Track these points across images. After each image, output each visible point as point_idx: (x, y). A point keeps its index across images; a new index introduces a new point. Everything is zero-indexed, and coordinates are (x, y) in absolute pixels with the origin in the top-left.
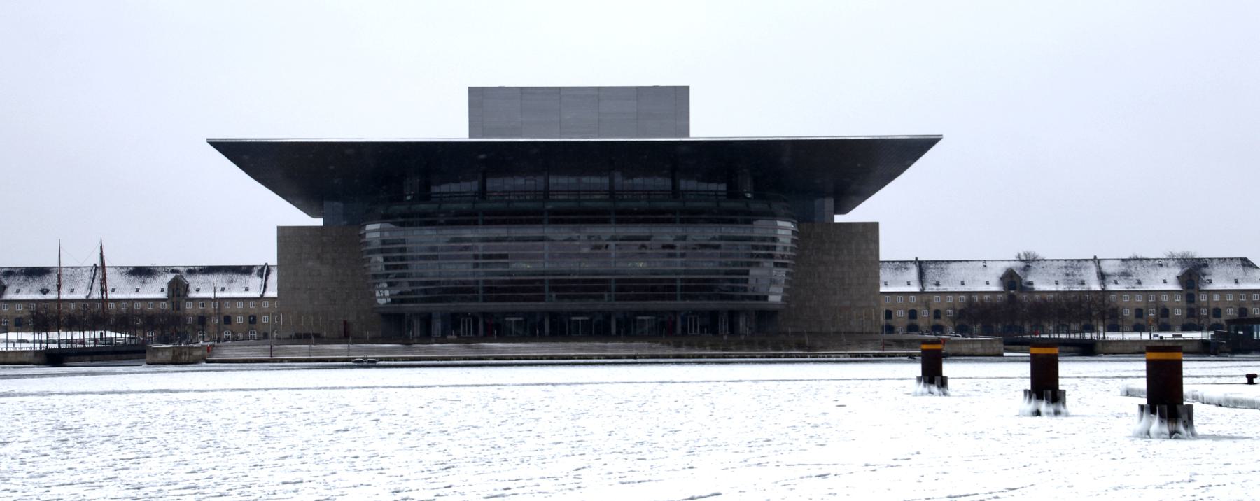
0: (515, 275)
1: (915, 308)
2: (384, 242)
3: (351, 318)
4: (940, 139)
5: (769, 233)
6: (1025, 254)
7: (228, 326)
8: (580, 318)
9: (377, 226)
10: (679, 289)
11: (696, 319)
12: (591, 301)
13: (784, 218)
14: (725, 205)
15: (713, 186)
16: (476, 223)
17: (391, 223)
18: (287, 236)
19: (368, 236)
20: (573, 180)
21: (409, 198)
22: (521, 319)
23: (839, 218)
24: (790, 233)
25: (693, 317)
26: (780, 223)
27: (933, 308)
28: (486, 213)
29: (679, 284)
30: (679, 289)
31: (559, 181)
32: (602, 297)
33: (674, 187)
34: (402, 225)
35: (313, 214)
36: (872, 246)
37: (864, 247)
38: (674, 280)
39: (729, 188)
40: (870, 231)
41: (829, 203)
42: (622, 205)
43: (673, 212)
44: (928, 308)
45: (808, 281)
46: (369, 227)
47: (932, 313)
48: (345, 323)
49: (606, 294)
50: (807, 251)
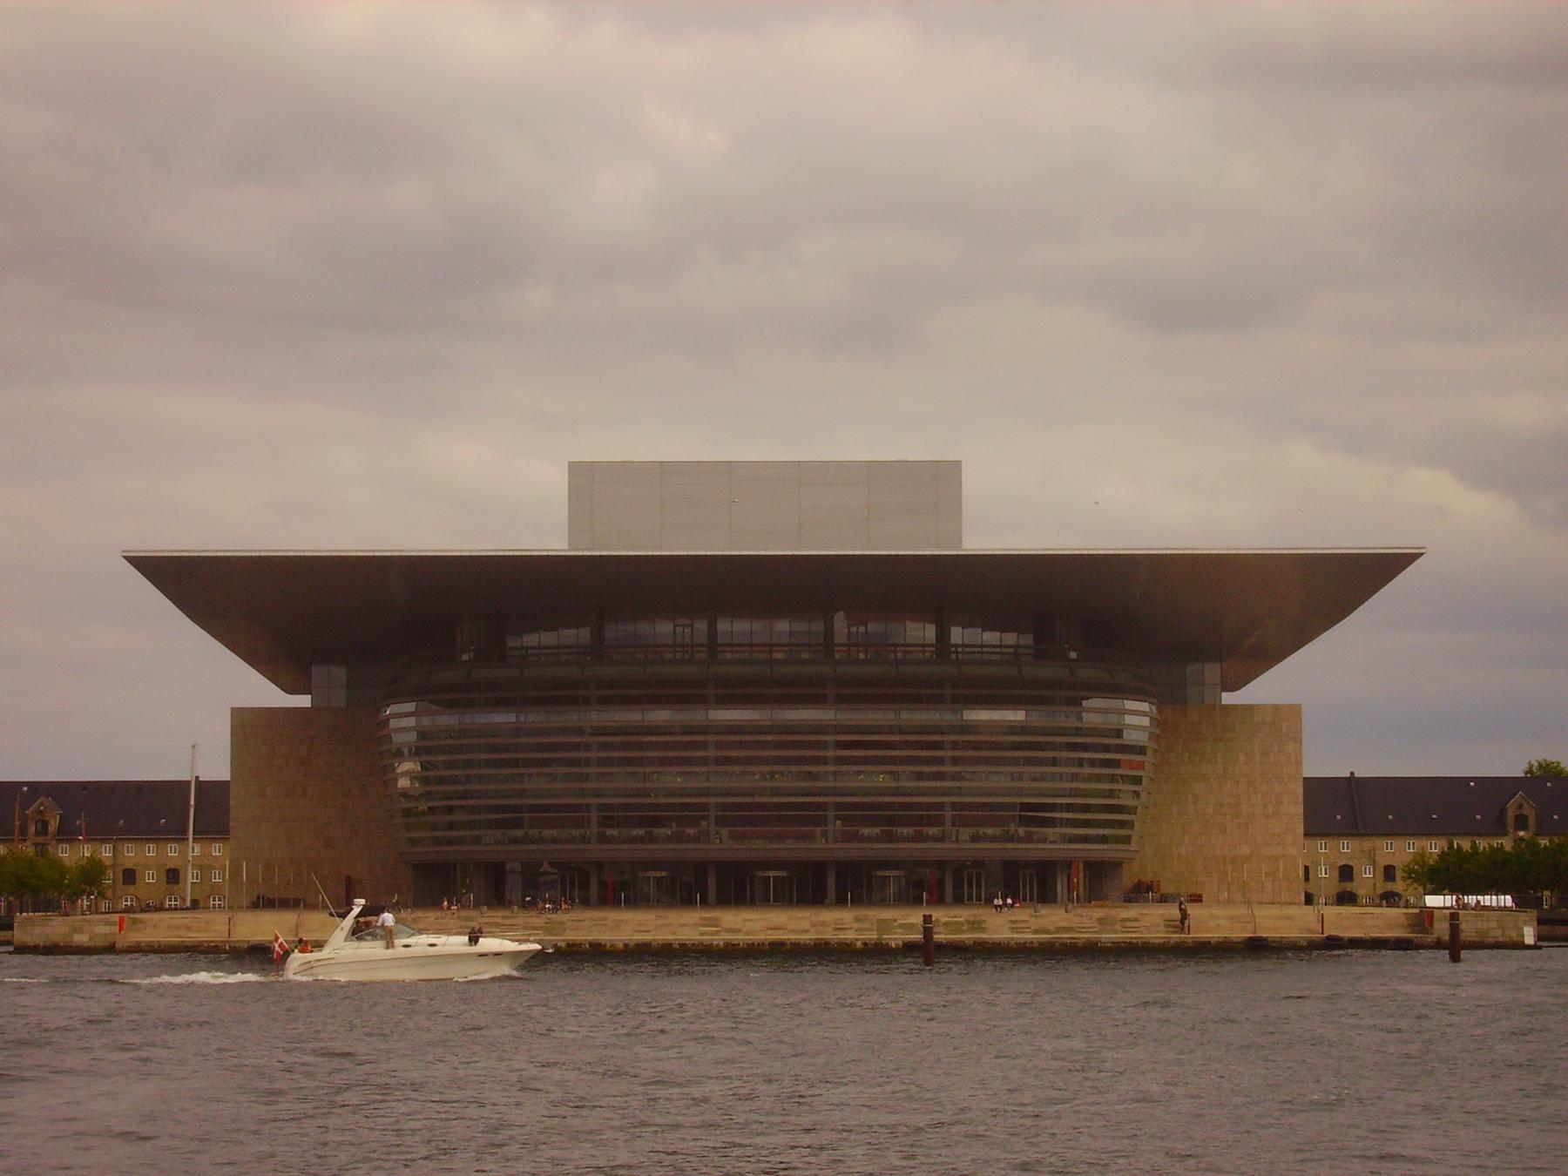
0: (656, 796)
1: (1351, 864)
2: (423, 735)
4: (1423, 554)
5: (1112, 721)
6: (1540, 766)
7: (131, 888)
8: (771, 874)
9: (410, 707)
10: (948, 824)
12: (790, 844)
13: (1139, 694)
15: (1011, 638)
16: (586, 701)
17: (433, 702)
19: (393, 723)
20: (758, 626)
21: (465, 657)
22: (664, 874)
23: (1228, 698)
24: (1146, 721)
26: (1130, 705)
27: (1383, 862)
31: (733, 628)
32: (810, 837)
33: (942, 636)
34: (451, 705)
35: (290, 690)
38: (940, 806)
39: (1036, 640)
40: (1284, 720)
41: (1212, 671)
44: (1374, 863)
47: (1380, 871)
49: (818, 830)
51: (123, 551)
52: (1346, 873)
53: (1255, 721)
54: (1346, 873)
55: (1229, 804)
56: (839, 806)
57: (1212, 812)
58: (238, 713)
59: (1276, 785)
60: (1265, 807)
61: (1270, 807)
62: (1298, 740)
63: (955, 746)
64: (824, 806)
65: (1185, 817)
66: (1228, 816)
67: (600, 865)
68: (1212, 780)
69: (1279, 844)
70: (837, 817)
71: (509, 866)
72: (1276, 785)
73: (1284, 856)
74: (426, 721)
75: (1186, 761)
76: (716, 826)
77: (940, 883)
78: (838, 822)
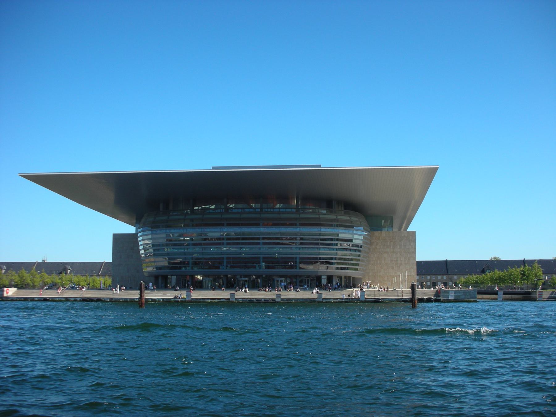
1: (446, 282)
9: (141, 230)
11: (308, 280)
28: (192, 220)
29: (298, 260)
32: (255, 267)
36: (412, 244)
37: (408, 244)
42: (263, 216)
43: (296, 219)
45: (379, 262)
49: (257, 265)
50: (378, 247)
51: (19, 174)
53: (402, 236)
55: (395, 260)
56: (264, 258)
57: (389, 263)
59: (408, 254)
60: (405, 261)
61: (407, 261)
62: (415, 242)
64: (259, 258)
65: (382, 264)
66: (394, 264)
68: (389, 253)
69: (410, 272)
70: (264, 262)
72: (408, 254)
73: (410, 275)
74: (145, 233)
75: (382, 248)
76: (227, 264)
77: (296, 283)
78: (264, 264)
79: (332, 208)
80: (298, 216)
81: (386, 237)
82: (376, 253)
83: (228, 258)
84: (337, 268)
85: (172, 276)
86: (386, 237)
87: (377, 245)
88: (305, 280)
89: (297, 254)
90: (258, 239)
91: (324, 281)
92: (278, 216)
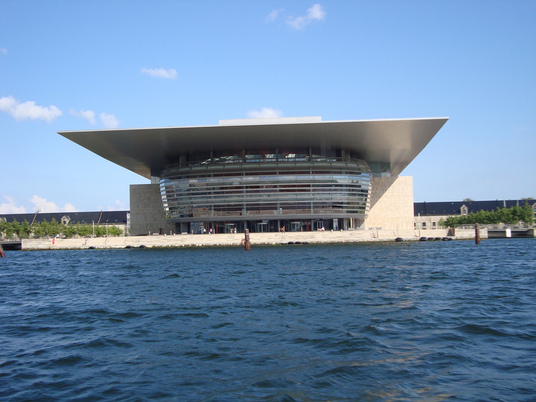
3: (163, 227)
6: (467, 200)
9: (163, 180)
10: (312, 207)
14: (333, 164)
16: (209, 176)
18: (135, 190)
25: (320, 222)
30: (312, 207)
38: (310, 203)
42: (280, 165)
43: (309, 168)
44: (430, 222)
46: (161, 181)
48: (160, 228)
50: (378, 191)
52: (424, 224)
54: (424, 224)
56: (281, 204)
58: (131, 186)
63: (313, 186)
64: (276, 204)
67: (215, 222)
70: (280, 207)
71: (191, 224)
75: (381, 192)
77: (310, 226)
78: (281, 209)
79: (341, 157)
80: (311, 165)
81: (385, 182)
82: (376, 197)
83: (247, 205)
84: (348, 212)
85: (194, 222)
86: (385, 182)
87: (377, 190)
88: (319, 223)
89: (311, 199)
90: (309, 186)
91: (335, 224)
92: (294, 165)
